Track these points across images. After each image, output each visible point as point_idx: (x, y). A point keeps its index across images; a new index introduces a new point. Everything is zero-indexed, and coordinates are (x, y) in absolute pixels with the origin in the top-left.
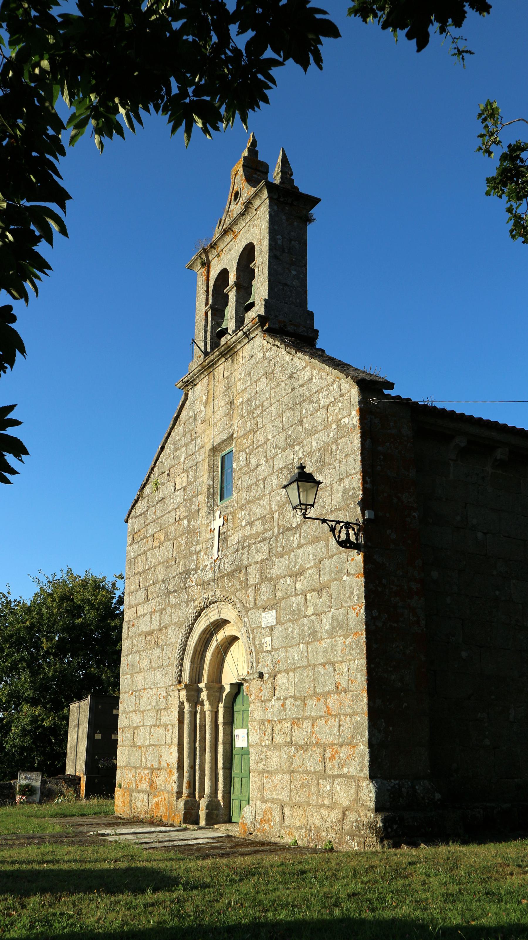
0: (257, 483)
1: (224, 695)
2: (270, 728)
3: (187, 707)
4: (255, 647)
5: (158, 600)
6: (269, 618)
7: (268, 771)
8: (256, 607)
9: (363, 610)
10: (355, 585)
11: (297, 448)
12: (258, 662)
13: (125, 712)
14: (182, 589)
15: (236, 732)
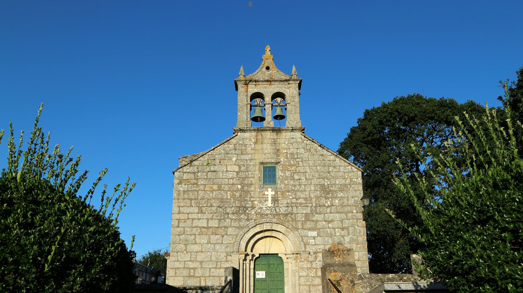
0: (300, 185)
1: (254, 258)
2: (314, 270)
3: (241, 261)
4: (304, 243)
5: (215, 215)
6: (314, 233)
7: (313, 285)
8: (303, 228)
9: (366, 237)
10: (364, 231)
11: (326, 180)
12: (305, 248)
13: (178, 261)
14: (242, 214)
15: (257, 272)
